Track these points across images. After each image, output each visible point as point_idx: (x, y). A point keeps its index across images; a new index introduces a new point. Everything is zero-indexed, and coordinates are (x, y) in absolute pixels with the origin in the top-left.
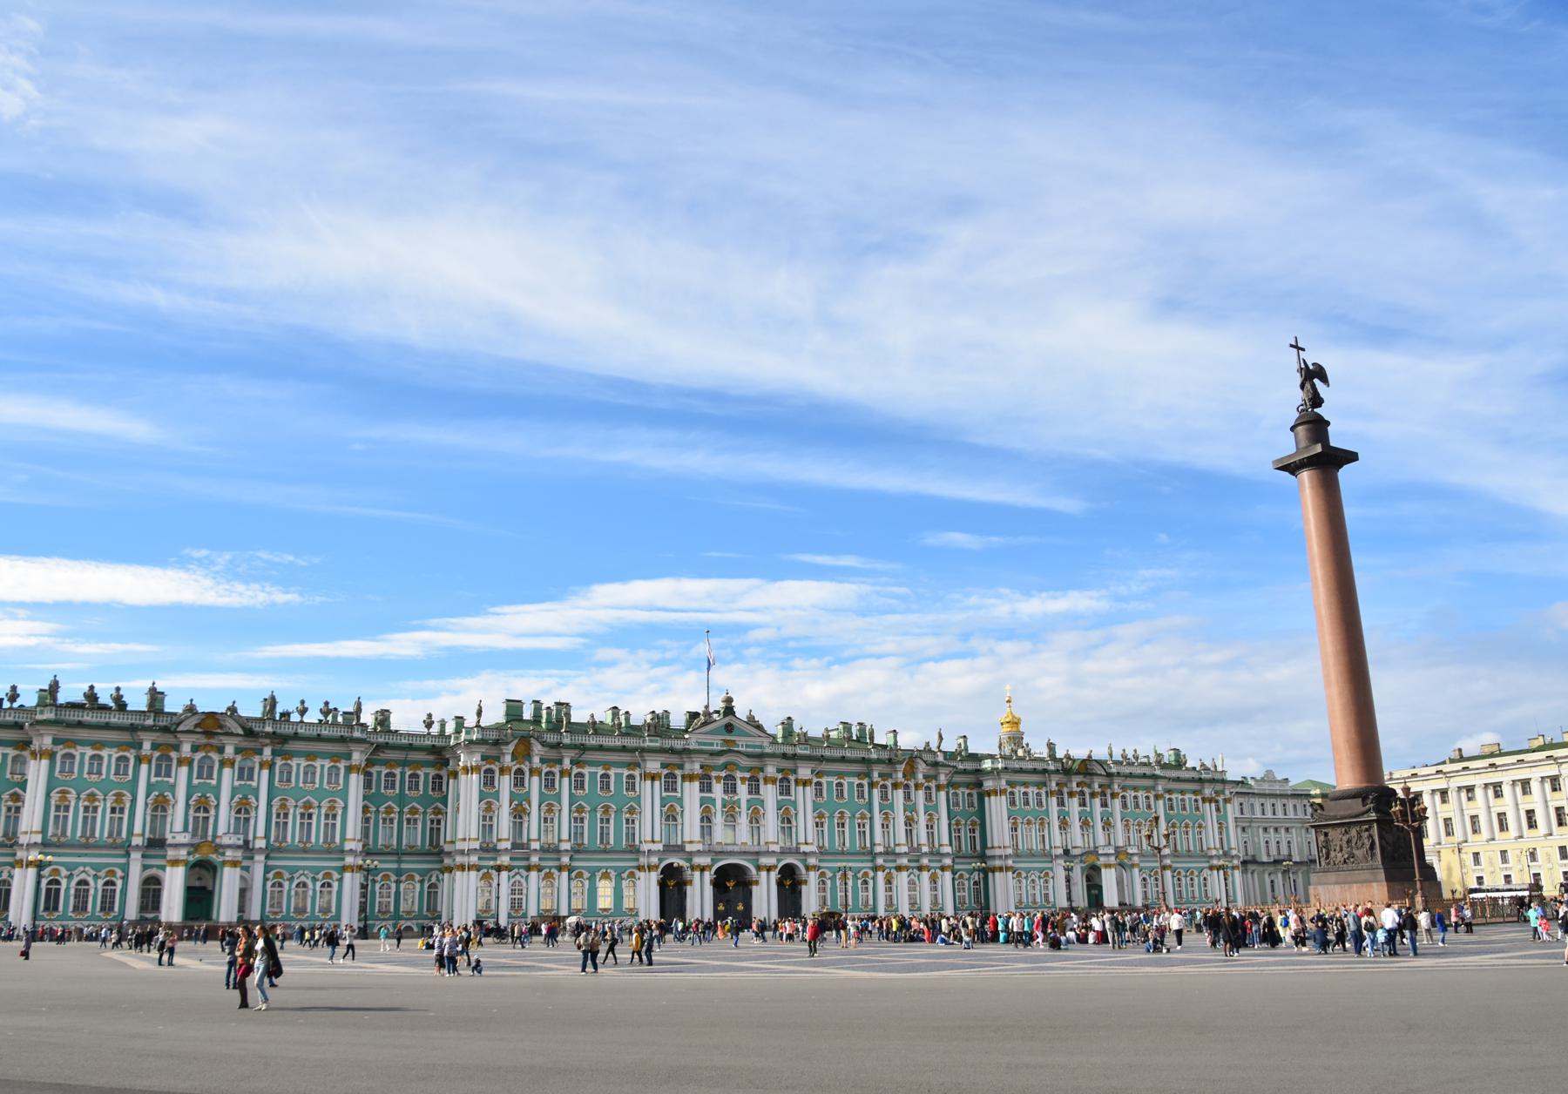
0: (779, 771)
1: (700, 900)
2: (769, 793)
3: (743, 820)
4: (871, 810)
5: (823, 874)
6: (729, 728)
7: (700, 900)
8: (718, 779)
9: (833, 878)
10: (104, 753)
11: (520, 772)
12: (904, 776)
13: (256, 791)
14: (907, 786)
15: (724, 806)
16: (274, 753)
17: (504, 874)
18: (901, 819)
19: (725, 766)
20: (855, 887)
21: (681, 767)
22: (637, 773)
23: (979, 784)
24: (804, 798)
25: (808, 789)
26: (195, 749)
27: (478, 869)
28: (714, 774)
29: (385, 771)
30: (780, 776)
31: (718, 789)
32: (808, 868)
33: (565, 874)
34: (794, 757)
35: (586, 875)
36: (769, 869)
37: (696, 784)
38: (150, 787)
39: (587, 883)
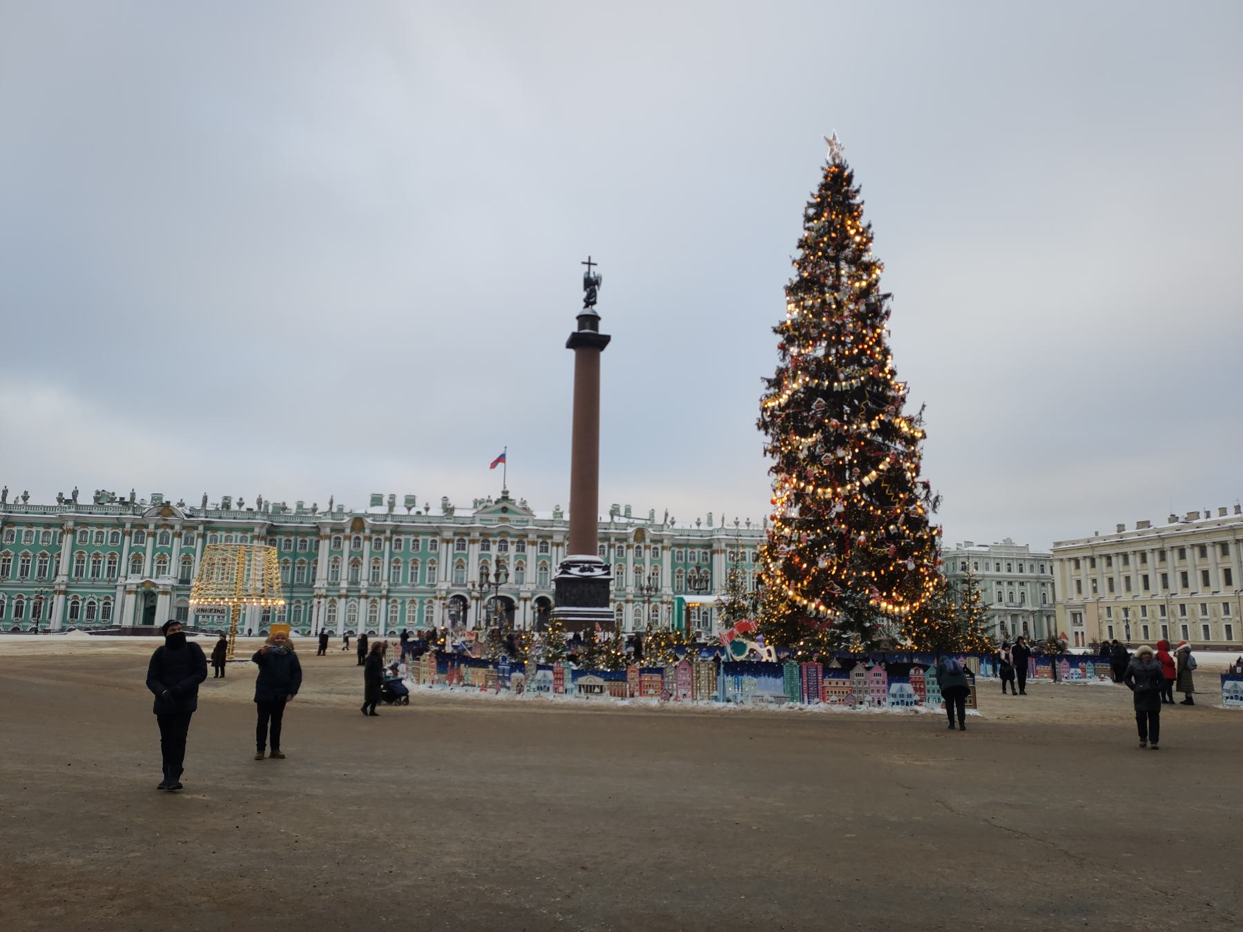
8: (494, 542)
10: (104, 530)
11: (358, 538)
13: (194, 551)
14: (638, 547)
16: (206, 529)
17: (343, 600)
18: (631, 569)
21: (468, 535)
22: (437, 538)
23: (710, 546)
25: (560, 548)
26: (157, 527)
27: (326, 597)
28: (491, 539)
29: (284, 538)
31: (494, 550)
33: (384, 601)
35: (399, 601)
37: (477, 547)
38: (131, 549)
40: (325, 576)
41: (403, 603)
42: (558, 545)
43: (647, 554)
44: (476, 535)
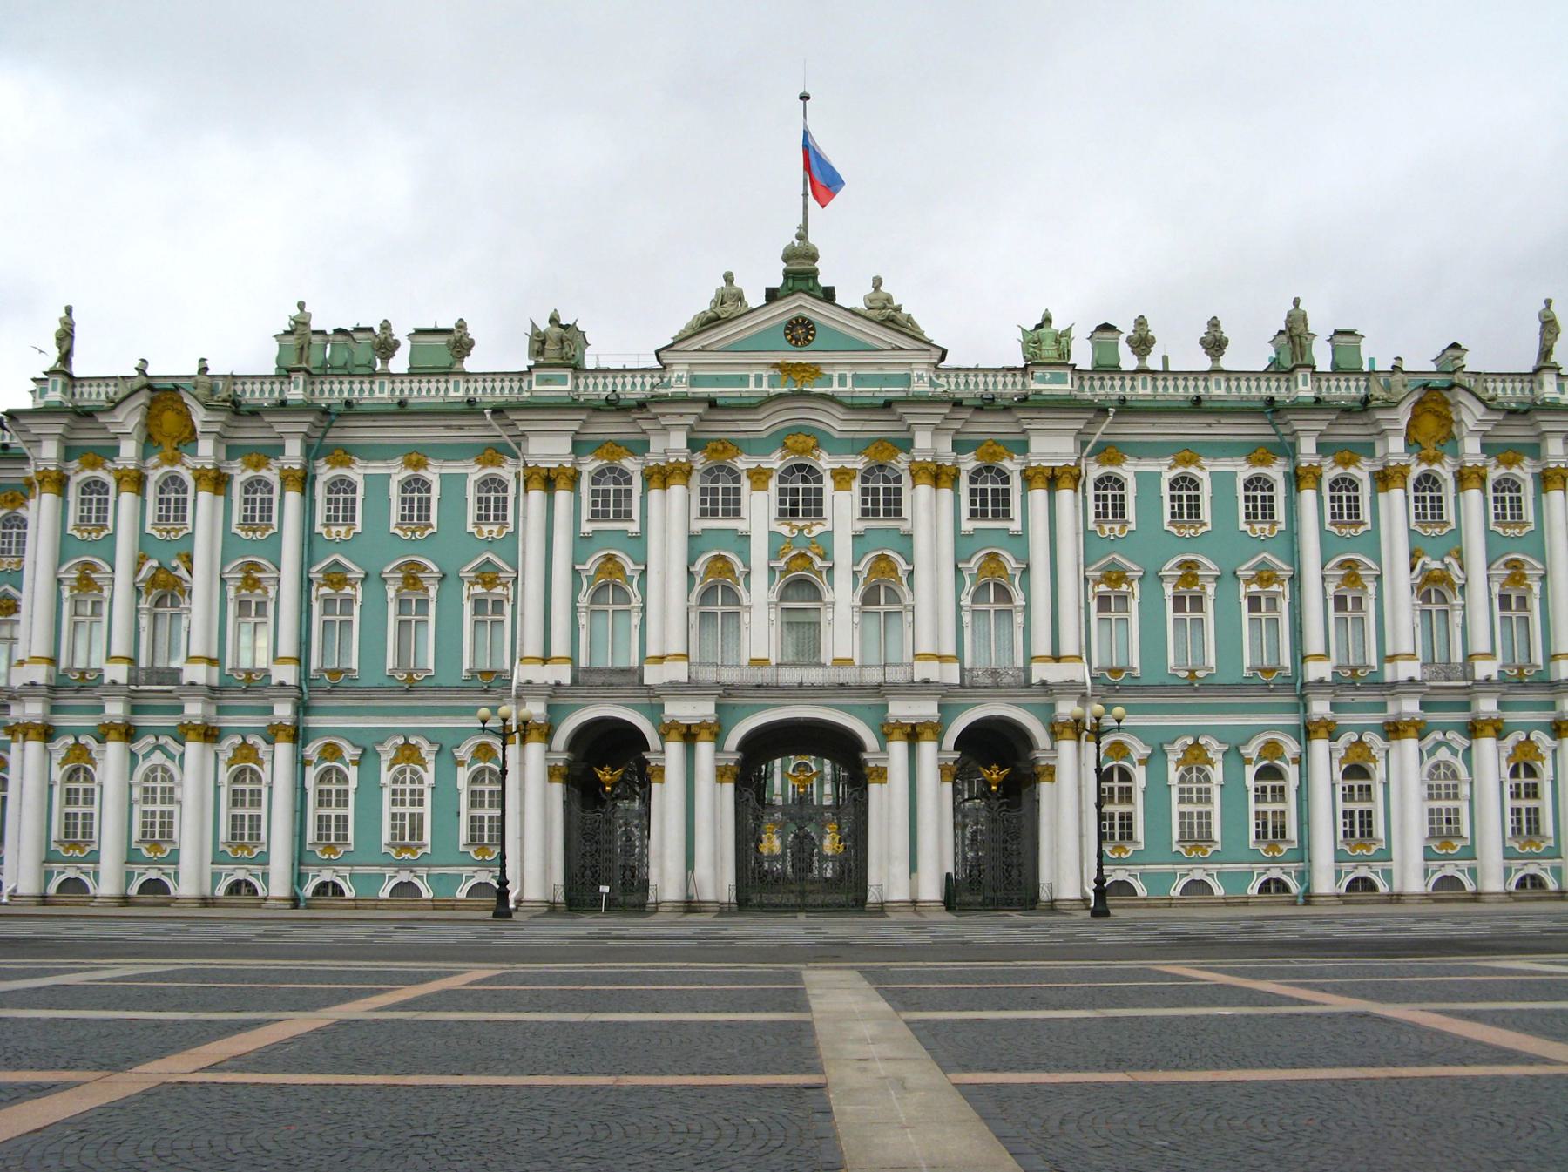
0: (958, 447)
1: (689, 833)
2: (931, 515)
3: (842, 594)
4: (1294, 556)
5: (1120, 749)
6: (800, 331)
7: (689, 833)
8: (759, 477)
9: (1156, 759)
11: (173, 481)
12: (1412, 442)
14: (1428, 481)
15: (775, 554)
18: (1401, 579)
19: (781, 439)
20: (1233, 787)
21: (640, 448)
22: (507, 471)
24: (1053, 527)
25: (1065, 496)
28: (742, 463)
30: (969, 463)
31: (760, 510)
32: (1055, 732)
33: (283, 750)
34: (1025, 402)
35: (350, 752)
36: (913, 735)
39: (352, 773)
40: (41, 648)
41: (367, 757)
42: (1053, 480)
43: (1472, 512)
44: (672, 444)
